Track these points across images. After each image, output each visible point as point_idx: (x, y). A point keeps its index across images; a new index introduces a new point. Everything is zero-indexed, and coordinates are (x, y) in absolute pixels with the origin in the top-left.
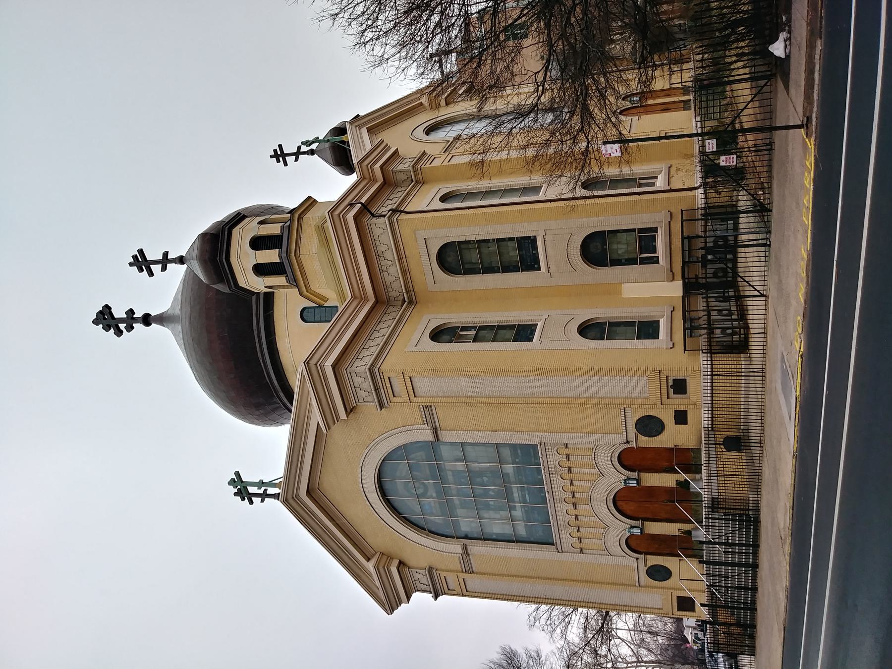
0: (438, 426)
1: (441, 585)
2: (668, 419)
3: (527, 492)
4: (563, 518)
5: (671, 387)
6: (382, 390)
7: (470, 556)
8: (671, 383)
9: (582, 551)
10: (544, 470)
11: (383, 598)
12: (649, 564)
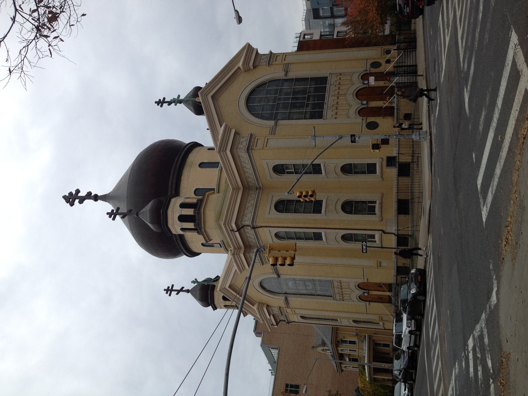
0: (289, 71)
1: (253, 143)
2: (383, 61)
3: (316, 98)
4: (332, 93)
5: (385, 52)
6: (272, 59)
7: (277, 127)
8: (385, 50)
9: (336, 118)
10: (328, 87)
11: (219, 143)
12: (368, 121)
